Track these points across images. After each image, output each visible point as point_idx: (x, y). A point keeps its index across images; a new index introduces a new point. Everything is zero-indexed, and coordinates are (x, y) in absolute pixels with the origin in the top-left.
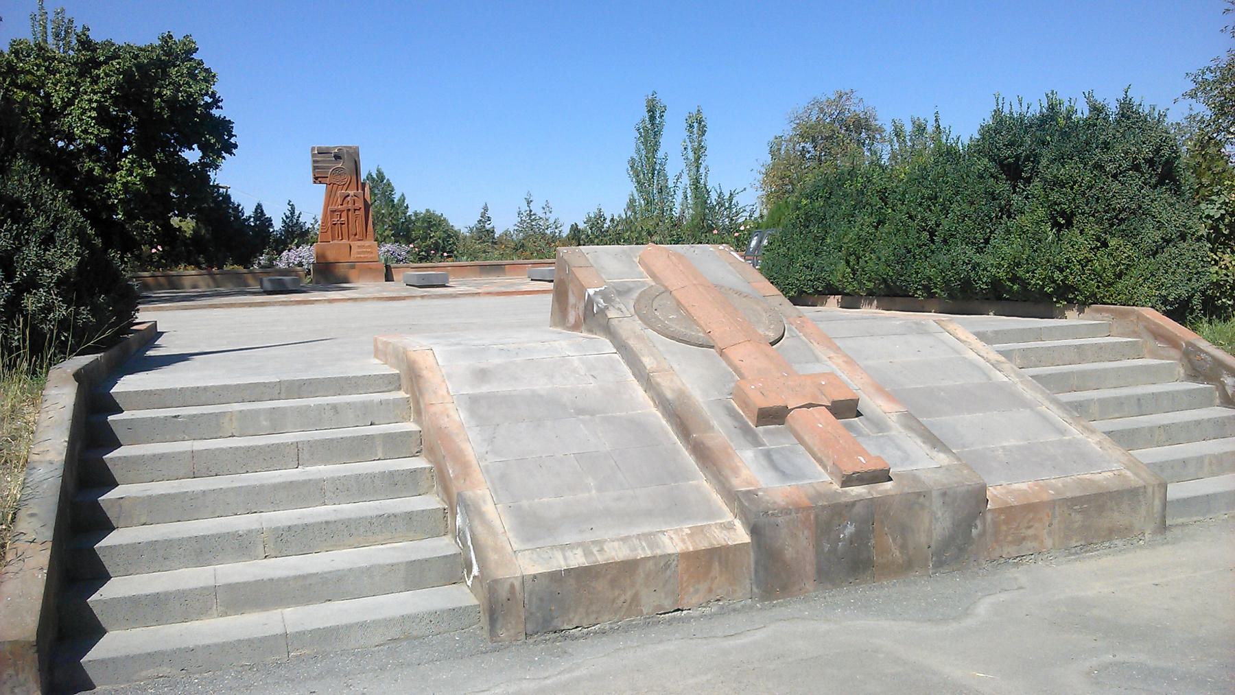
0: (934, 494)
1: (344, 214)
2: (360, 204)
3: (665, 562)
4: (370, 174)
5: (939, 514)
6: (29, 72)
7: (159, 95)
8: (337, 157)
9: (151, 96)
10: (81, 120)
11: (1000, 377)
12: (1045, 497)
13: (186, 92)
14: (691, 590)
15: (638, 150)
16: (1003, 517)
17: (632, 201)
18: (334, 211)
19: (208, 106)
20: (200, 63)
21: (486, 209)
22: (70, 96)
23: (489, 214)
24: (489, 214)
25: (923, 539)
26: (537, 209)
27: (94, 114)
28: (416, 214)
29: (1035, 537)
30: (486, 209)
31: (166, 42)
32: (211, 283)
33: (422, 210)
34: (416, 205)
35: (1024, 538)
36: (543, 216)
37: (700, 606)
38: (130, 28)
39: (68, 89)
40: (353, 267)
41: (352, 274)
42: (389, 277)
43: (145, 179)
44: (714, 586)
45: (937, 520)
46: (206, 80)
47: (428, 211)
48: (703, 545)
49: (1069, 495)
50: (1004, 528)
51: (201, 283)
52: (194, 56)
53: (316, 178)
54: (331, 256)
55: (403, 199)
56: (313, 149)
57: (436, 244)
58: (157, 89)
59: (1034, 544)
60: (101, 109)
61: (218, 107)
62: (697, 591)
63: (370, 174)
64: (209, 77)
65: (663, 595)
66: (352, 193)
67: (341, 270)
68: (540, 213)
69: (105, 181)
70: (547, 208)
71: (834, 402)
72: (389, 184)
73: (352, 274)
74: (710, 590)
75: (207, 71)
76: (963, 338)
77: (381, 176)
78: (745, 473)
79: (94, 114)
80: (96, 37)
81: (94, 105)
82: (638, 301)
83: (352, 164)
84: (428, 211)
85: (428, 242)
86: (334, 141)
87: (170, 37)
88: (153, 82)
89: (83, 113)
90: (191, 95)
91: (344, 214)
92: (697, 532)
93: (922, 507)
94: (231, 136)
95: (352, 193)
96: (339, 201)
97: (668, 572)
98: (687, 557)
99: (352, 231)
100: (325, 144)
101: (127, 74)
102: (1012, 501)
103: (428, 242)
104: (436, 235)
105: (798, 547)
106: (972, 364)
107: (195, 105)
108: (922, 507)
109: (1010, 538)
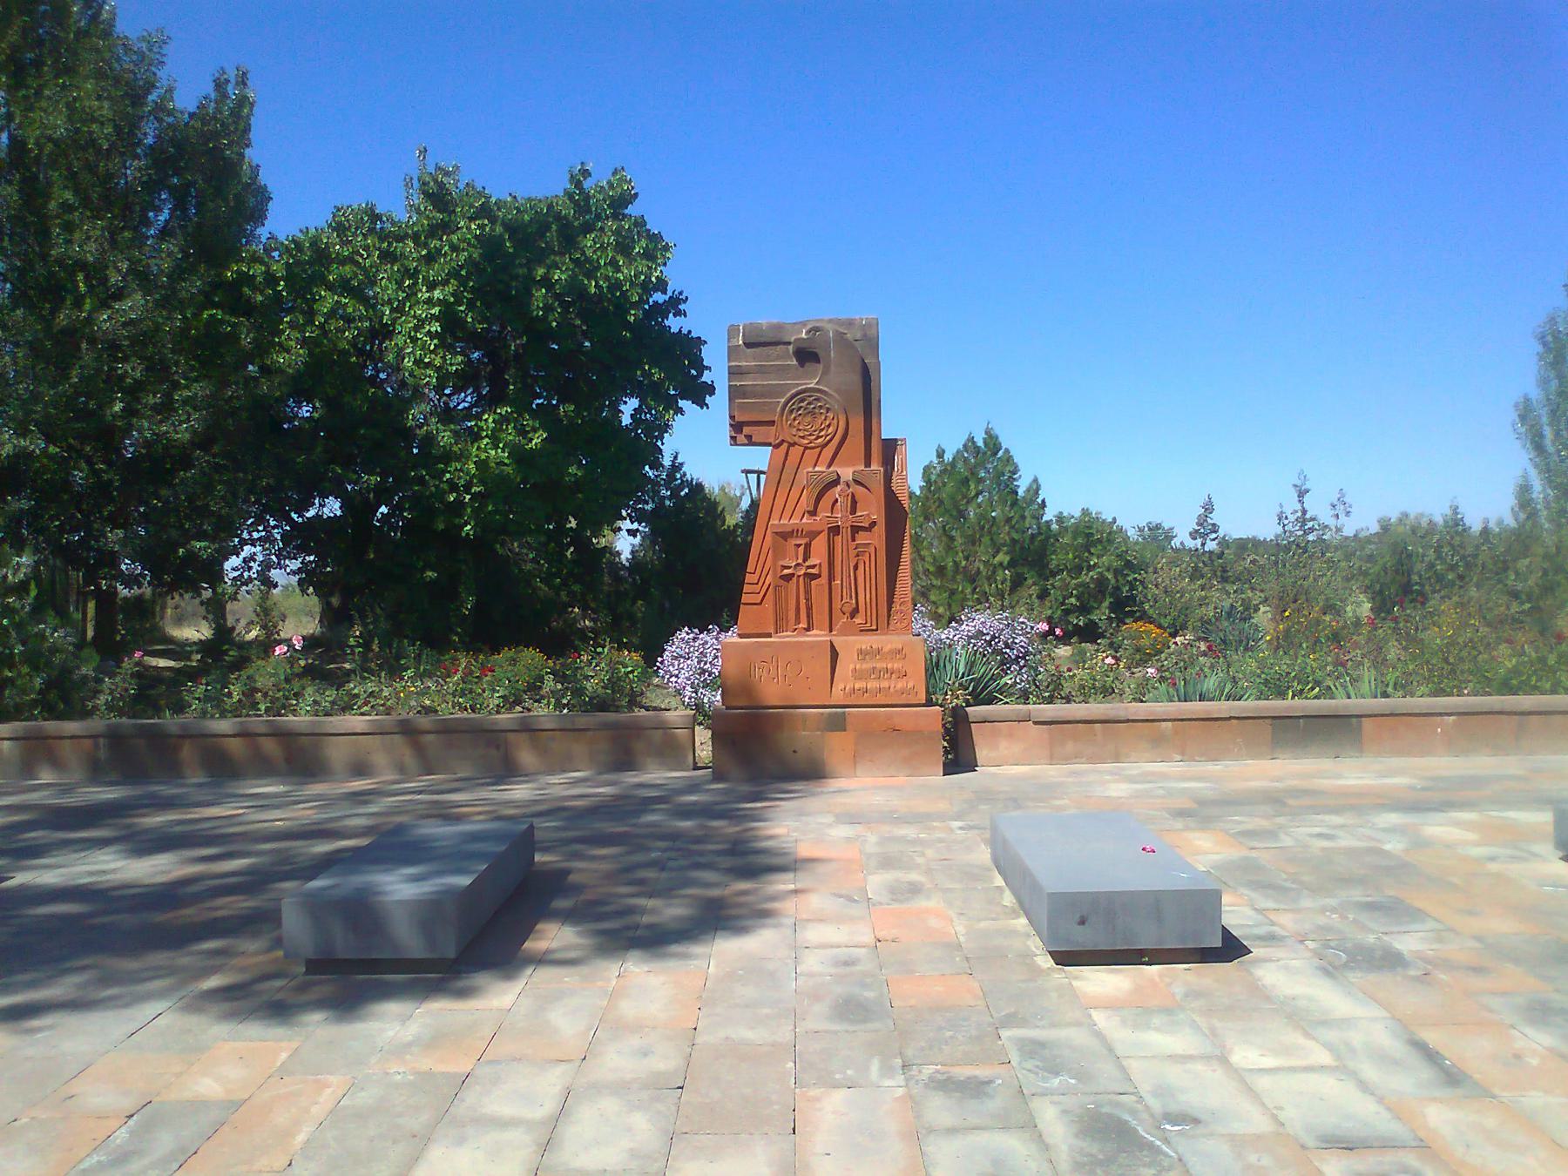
1: (820, 545)
2: (872, 510)
4: (971, 439)
6: (350, 260)
7: (546, 281)
8: (806, 355)
9: (530, 283)
10: (414, 340)
13: (607, 278)
15: (1544, 382)
17: (1524, 490)
18: (785, 535)
19: (661, 310)
20: (640, 223)
21: (1208, 508)
22: (402, 295)
23: (1215, 518)
24: (1215, 518)
26: (1319, 508)
27: (435, 327)
28: (1060, 519)
30: (1208, 508)
31: (578, 184)
32: (409, 759)
33: (1073, 510)
34: (1062, 500)
36: (1332, 522)
38: (520, 171)
39: (400, 284)
40: (837, 724)
41: (835, 747)
42: (959, 758)
43: (521, 457)
46: (649, 255)
47: (1085, 512)
51: (380, 759)
52: (630, 210)
53: (737, 427)
54: (771, 691)
55: (1035, 488)
56: (732, 331)
57: (1101, 582)
58: (541, 271)
60: (450, 320)
61: (678, 313)
63: (971, 439)
64: (656, 249)
66: (847, 473)
67: (803, 736)
68: (1325, 517)
69: (448, 457)
70: (1341, 505)
72: (1009, 459)
73: (835, 747)
75: (656, 238)
77: (993, 443)
79: (435, 327)
80: (456, 186)
81: (436, 310)
83: (855, 379)
84: (1085, 512)
85: (1085, 577)
86: (797, 307)
87: (586, 173)
88: (540, 257)
89: (417, 328)
90: (617, 285)
91: (820, 545)
94: (702, 368)
95: (847, 473)
96: (806, 502)
99: (844, 602)
100: (765, 317)
101: (490, 245)
103: (1085, 577)
104: (1103, 562)
107: (622, 306)
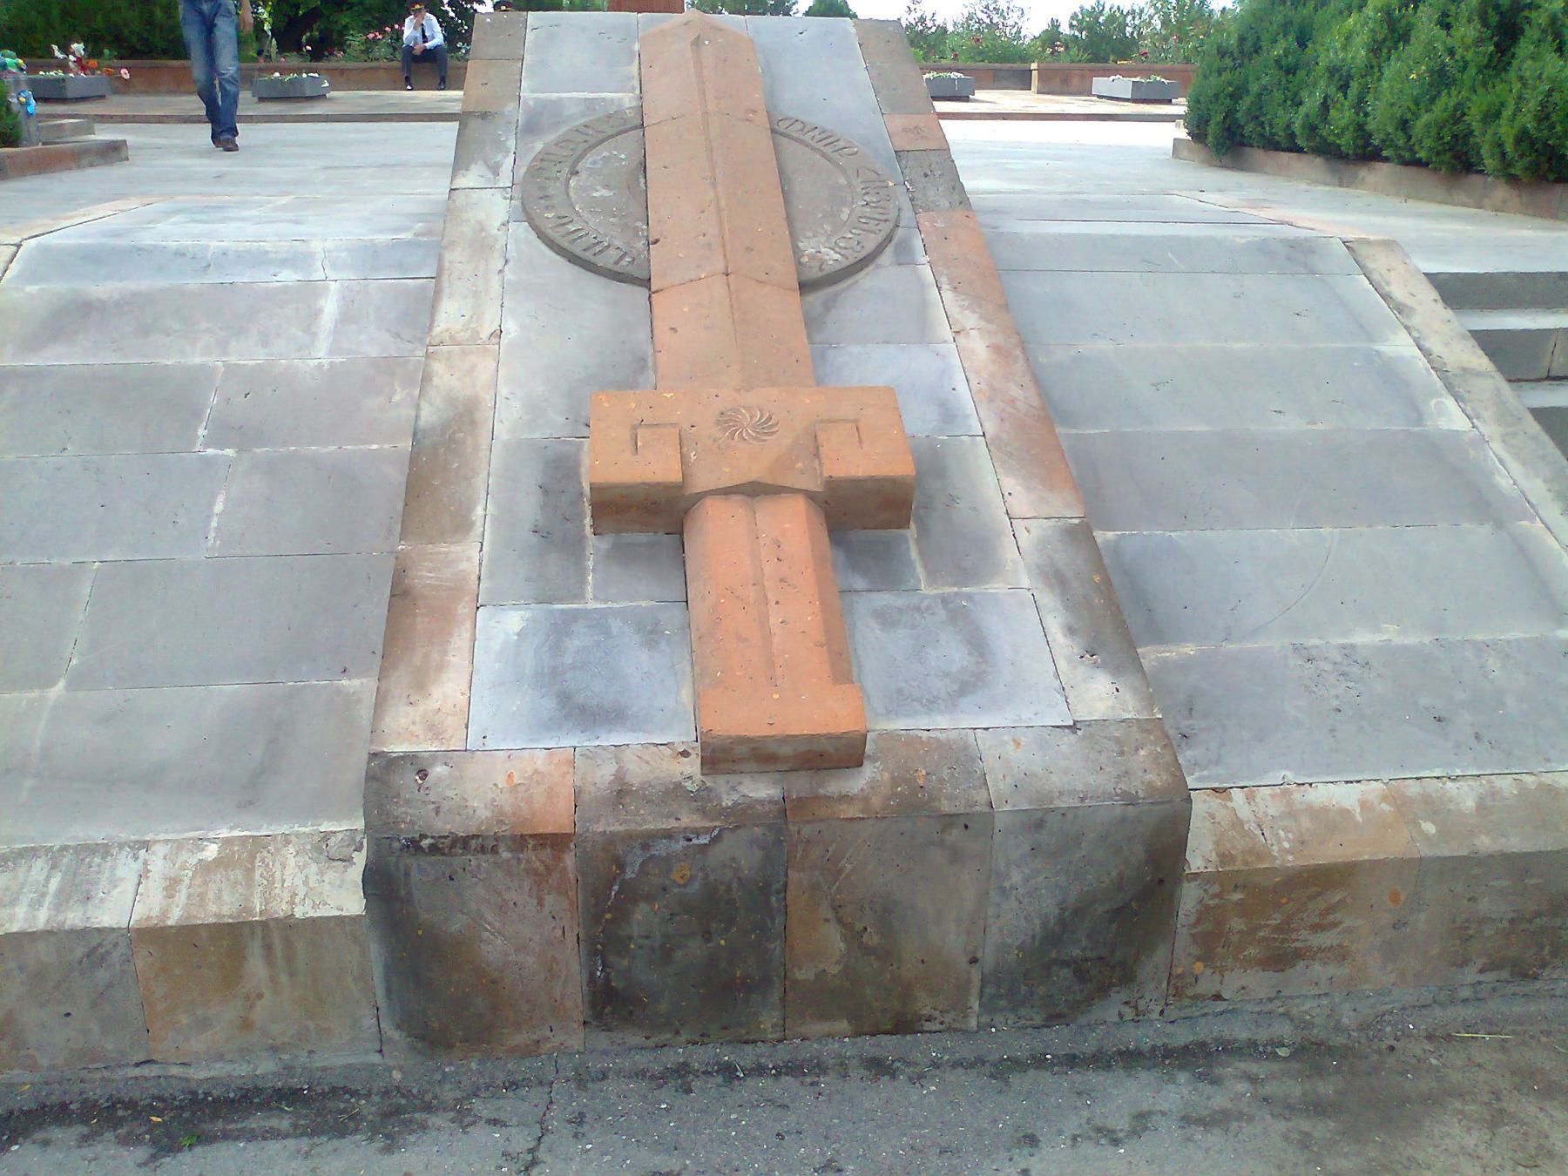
0: (999, 823)
3: (92, 948)
5: (1016, 877)
11: (1450, 417)
12: (1397, 845)
14: (185, 1020)
16: (1237, 896)
25: (951, 940)
29: (1341, 955)
35: (1298, 955)
37: (220, 1057)
44: (258, 1013)
45: (1004, 892)
48: (221, 905)
49: (1486, 843)
50: (1237, 924)
59: (1332, 970)
62: (203, 1024)
65: (94, 1027)
71: (832, 484)
74: (246, 1024)
76: (1398, 293)
78: (448, 690)
82: (543, 157)
92: (244, 857)
93: (956, 856)
97: (102, 975)
98: (152, 936)
102: (1283, 850)
105: (522, 935)
106: (1389, 374)
108: (956, 856)
109: (1252, 951)
